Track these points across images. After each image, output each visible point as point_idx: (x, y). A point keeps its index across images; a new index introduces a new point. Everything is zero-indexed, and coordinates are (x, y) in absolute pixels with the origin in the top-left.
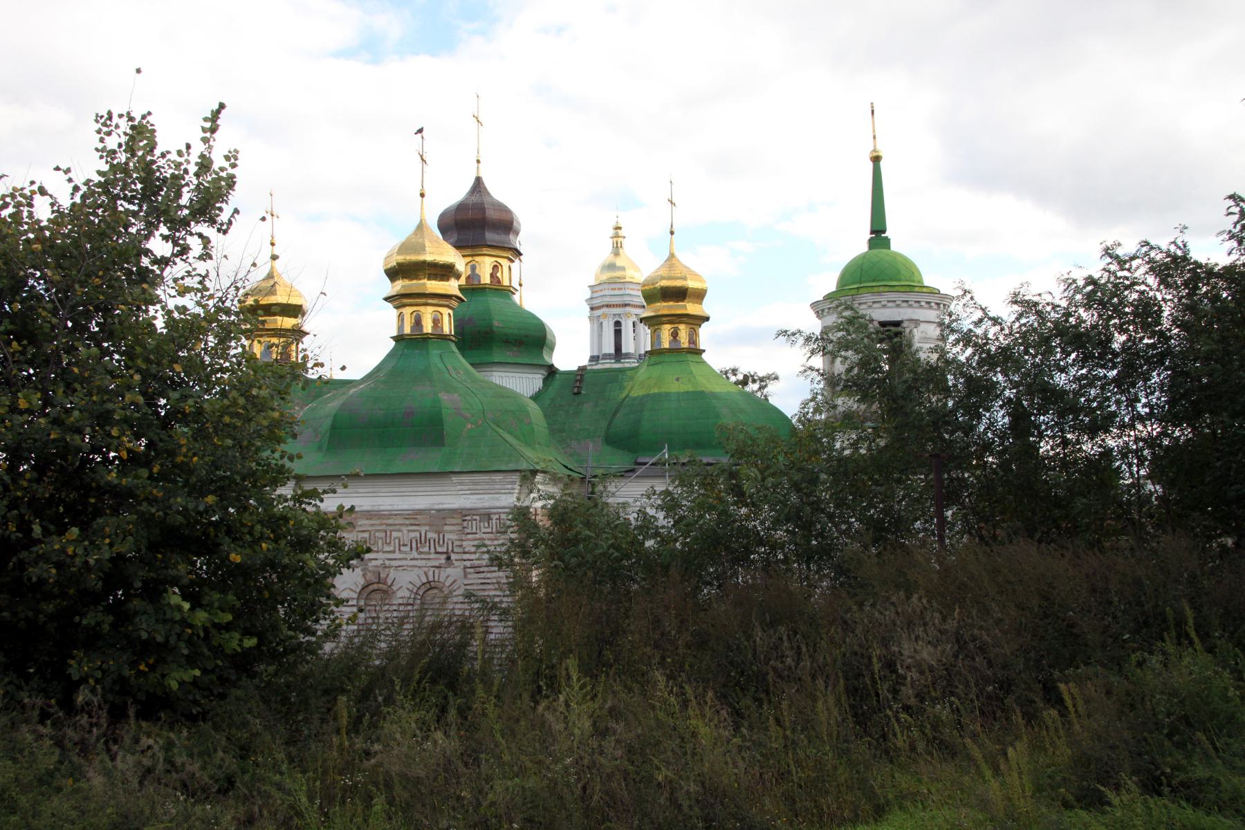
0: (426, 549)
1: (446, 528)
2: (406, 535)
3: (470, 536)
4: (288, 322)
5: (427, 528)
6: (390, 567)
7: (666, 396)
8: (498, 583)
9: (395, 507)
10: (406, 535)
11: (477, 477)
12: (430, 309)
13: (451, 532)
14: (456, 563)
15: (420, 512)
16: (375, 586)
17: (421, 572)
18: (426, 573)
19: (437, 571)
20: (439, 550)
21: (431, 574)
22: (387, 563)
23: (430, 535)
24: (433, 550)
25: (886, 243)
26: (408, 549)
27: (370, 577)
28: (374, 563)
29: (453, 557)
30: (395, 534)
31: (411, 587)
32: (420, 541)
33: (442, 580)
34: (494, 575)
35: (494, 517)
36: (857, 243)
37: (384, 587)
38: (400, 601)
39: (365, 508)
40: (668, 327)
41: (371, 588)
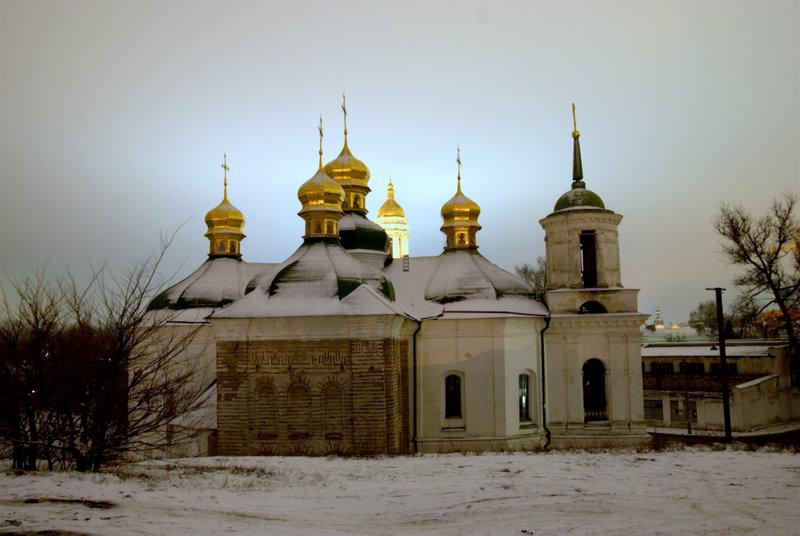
2: (318, 354)
10: (318, 354)
12: (326, 221)
25: (583, 185)
27: (295, 379)
28: (297, 371)
29: (345, 367)
36: (565, 185)
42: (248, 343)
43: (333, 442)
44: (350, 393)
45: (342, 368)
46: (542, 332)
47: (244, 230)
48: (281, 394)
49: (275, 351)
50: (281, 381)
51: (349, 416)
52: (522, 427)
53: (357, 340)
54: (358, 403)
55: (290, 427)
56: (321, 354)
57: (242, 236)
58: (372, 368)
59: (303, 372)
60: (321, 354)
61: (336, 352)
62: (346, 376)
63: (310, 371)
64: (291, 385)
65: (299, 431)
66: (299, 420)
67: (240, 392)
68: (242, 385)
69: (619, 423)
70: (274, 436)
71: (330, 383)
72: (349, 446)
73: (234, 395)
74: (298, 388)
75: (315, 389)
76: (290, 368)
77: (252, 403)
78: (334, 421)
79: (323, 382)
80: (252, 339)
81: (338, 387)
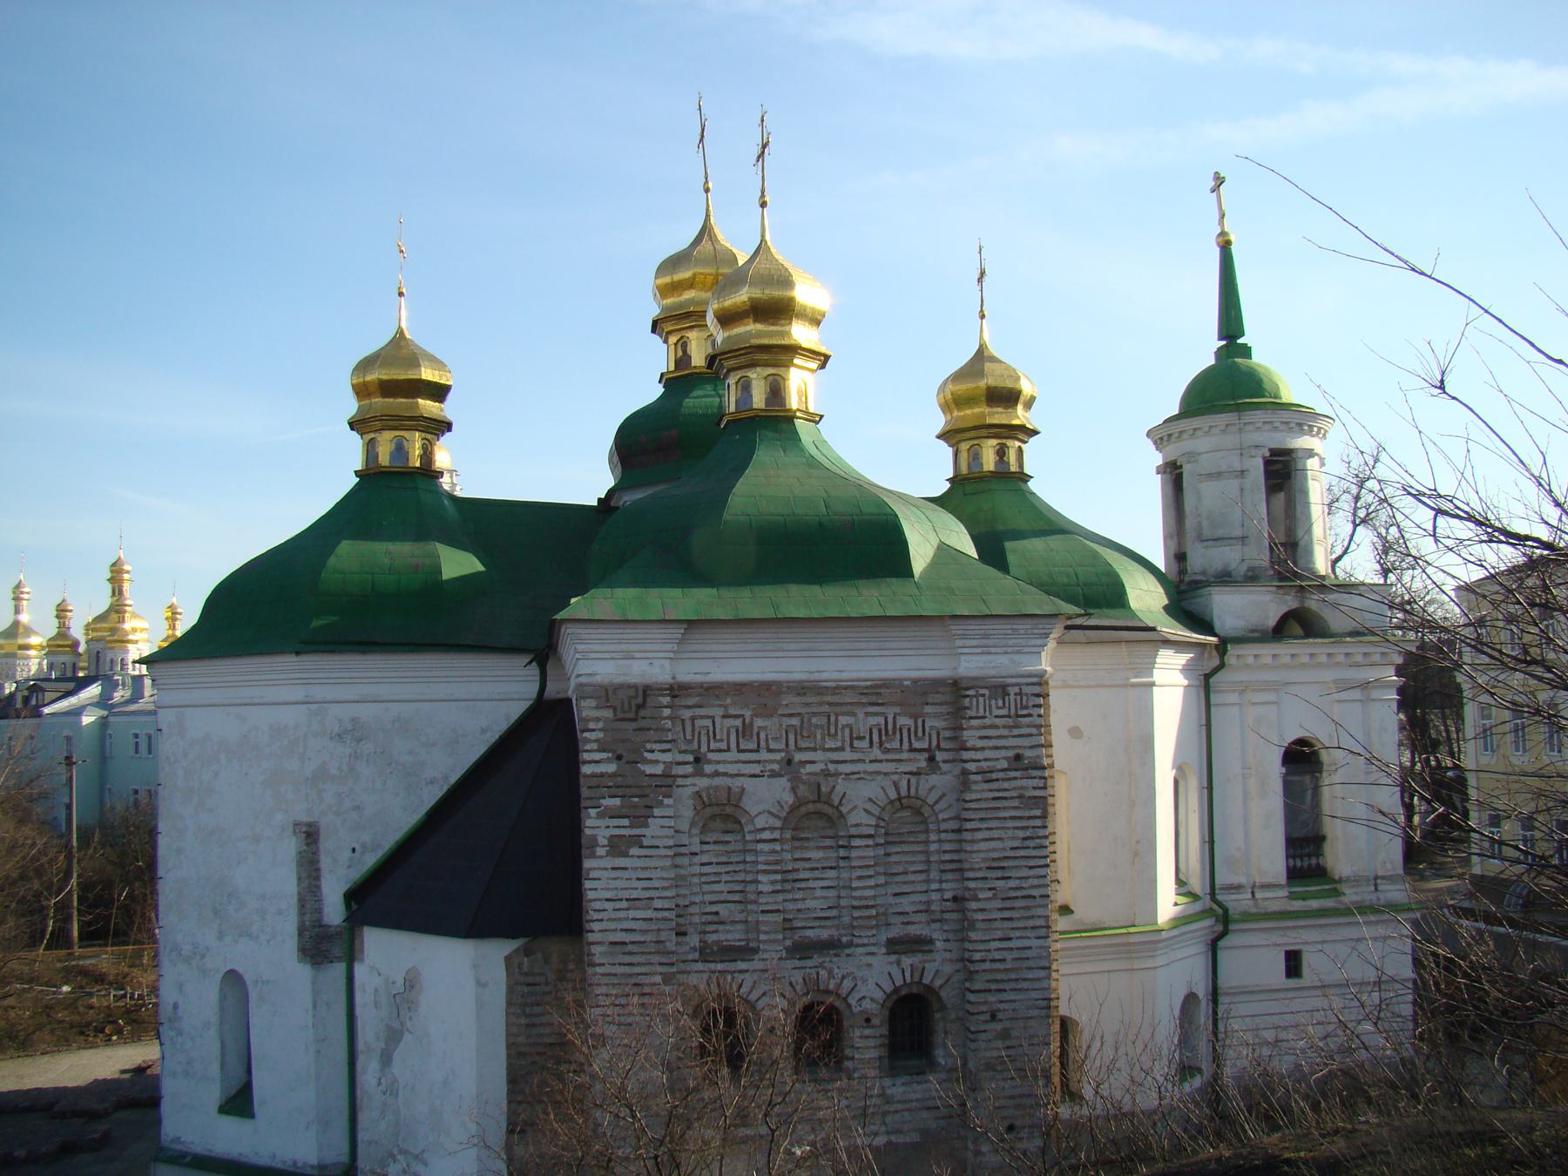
0: (896, 744)
1: (928, 709)
3: (974, 722)
4: (427, 406)
5: (898, 709)
6: (837, 774)
8: (1021, 797)
9: (845, 676)
10: (865, 721)
11: (989, 626)
13: (936, 715)
15: (886, 684)
16: (811, 807)
17: (888, 783)
18: (895, 784)
19: (913, 780)
20: (917, 745)
22: (832, 767)
23: (902, 721)
24: (906, 745)
26: (865, 744)
28: (809, 768)
29: (939, 756)
30: (843, 720)
31: (869, 806)
32: (884, 732)
33: (922, 793)
34: (1014, 784)
35: (1012, 691)
36: (1203, 352)
37: (829, 811)
38: (853, 831)
40: (994, 442)
41: (803, 810)
42: (677, 690)
43: (907, 961)
44: (953, 825)
45: (931, 759)
46: (1207, 677)
47: (447, 410)
48: (766, 835)
49: (748, 714)
50: (766, 797)
51: (950, 889)
52: (1292, 896)
53: (976, 683)
54: (981, 851)
55: (788, 926)
56: (873, 721)
57: (448, 426)
58: (1018, 757)
59: (826, 774)
60: (873, 721)
61: (915, 717)
63: (843, 768)
64: (793, 809)
65: (808, 933)
66: (810, 904)
67: (654, 829)
68: (656, 812)
69: (1356, 881)
70: (745, 951)
71: (900, 803)
72: (948, 969)
73: (637, 841)
74: (815, 813)
75: (859, 819)
76: (789, 762)
77: (685, 861)
78: (906, 904)
79: (883, 801)
80: (683, 678)
81: (918, 812)
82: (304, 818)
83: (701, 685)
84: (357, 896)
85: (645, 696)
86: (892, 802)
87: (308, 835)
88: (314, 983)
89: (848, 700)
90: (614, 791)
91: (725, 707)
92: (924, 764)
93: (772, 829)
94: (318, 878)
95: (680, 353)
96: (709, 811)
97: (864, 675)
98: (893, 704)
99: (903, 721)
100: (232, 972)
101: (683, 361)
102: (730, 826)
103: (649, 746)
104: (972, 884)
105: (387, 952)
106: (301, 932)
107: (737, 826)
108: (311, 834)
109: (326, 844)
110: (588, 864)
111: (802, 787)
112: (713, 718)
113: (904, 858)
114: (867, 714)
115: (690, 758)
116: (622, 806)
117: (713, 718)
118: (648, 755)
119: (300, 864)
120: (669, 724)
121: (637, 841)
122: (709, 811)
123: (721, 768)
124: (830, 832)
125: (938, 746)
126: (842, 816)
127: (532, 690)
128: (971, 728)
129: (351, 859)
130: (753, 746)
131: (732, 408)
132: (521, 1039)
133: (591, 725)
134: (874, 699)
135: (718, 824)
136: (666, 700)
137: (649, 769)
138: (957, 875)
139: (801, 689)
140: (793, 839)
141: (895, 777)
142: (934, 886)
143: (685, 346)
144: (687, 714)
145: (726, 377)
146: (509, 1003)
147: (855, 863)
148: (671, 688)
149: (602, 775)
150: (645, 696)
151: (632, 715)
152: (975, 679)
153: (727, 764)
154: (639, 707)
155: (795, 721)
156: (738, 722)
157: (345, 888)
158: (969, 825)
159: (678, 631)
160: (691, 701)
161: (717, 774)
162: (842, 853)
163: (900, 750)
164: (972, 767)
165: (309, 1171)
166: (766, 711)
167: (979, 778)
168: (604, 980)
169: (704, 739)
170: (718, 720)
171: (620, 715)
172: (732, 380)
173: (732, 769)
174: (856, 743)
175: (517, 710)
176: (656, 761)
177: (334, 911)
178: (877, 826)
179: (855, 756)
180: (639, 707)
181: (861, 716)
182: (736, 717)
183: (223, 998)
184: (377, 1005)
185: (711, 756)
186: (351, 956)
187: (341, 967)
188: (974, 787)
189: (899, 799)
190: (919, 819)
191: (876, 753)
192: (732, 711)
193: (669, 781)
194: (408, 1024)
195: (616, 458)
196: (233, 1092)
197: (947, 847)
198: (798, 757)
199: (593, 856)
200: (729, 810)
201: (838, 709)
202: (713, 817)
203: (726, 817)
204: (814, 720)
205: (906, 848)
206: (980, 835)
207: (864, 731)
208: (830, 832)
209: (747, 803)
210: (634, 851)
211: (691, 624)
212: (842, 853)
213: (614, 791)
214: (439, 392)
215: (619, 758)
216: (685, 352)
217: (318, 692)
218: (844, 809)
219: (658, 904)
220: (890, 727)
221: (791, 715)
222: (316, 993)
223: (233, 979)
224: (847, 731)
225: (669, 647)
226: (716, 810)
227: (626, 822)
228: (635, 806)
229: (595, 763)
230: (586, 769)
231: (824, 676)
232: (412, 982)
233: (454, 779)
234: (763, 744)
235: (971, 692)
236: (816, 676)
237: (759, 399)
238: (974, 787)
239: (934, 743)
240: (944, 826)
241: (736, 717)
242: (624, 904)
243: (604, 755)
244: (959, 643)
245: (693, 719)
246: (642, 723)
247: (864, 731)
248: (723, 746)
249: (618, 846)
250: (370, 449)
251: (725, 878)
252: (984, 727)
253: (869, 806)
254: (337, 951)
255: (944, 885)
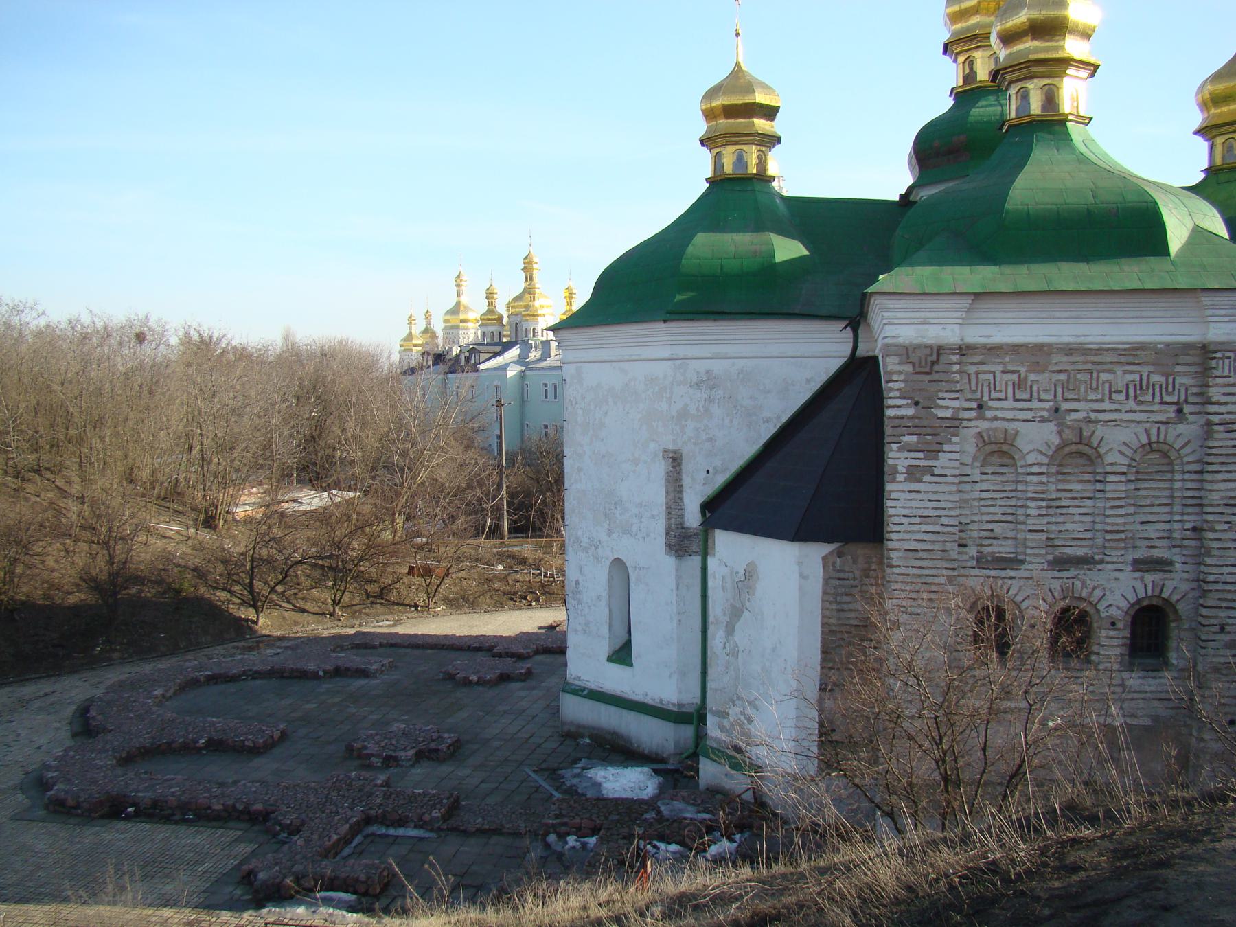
0: (1149, 398)
1: (1178, 369)
2: (1123, 378)
3: (1219, 381)
4: (761, 124)
5: (1151, 369)
6: (1097, 422)
7: (931, 263)
9: (1107, 339)
10: (1123, 378)
13: (1185, 374)
14: (1191, 418)
15: (1142, 347)
16: (1074, 448)
17: (1140, 429)
18: (1147, 431)
19: (1163, 428)
20: (1167, 399)
21: (1154, 432)
22: (1093, 416)
23: (1156, 378)
24: (1157, 399)
26: (1122, 397)
27: (1068, 434)
28: (1074, 416)
29: (1187, 409)
31: (1124, 449)
32: (1139, 387)
33: (1170, 439)
38: (1109, 469)
39: (1065, 340)
41: (1067, 450)
42: (964, 350)
43: (1149, 578)
44: (1196, 467)
45: (1180, 411)
48: (1035, 469)
49: (1023, 370)
50: (1035, 440)
51: (1191, 520)
55: (1050, 543)
56: (1129, 377)
60: (1129, 377)
61: (1167, 375)
62: (1188, 430)
64: (1059, 448)
65: (1068, 550)
66: (1069, 527)
67: (943, 462)
68: (946, 447)
70: (1013, 562)
71: (1150, 447)
72: (1185, 587)
73: (929, 470)
74: (1078, 453)
75: (1114, 459)
76: (1057, 410)
77: (968, 487)
80: (970, 339)
81: (1165, 455)
82: (671, 447)
83: (984, 346)
84: (709, 506)
85: (938, 354)
86: (1143, 446)
87: (674, 459)
88: (677, 570)
89: (1109, 360)
90: (912, 430)
91: (1004, 364)
92: (1172, 415)
93: (1041, 464)
94: (681, 492)
95: (967, 71)
96: (988, 448)
97: (1124, 339)
98: (1147, 364)
99: (1156, 378)
100: (618, 559)
101: (970, 77)
102: (1006, 461)
103: (940, 395)
104: (1210, 518)
105: (732, 549)
106: (667, 534)
107: (1010, 461)
108: (675, 460)
109: (687, 466)
110: (889, 487)
111: (1067, 431)
112: (994, 373)
113: (1152, 493)
114: (1125, 372)
115: (975, 405)
116: (918, 443)
117: (994, 373)
118: (940, 402)
119: (668, 481)
120: (957, 377)
121: (929, 470)
122: (988, 448)
123: (999, 414)
124: (1089, 469)
125: (1186, 401)
126: (1100, 456)
127: (846, 349)
128: (1217, 385)
129: (706, 479)
130: (1027, 396)
131: (1013, 115)
132: (833, 621)
133: (895, 378)
134: (1131, 359)
135: (995, 459)
136: (955, 358)
137: (940, 413)
138: (1197, 510)
139: (1069, 350)
140: (1058, 473)
141: (1148, 425)
142: (1177, 517)
143: (971, 64)
144: (972, 369)
145: (1007, 89)
146: (825, 593)
147: (1108, 495)
148: (960, 348)
149: (902, 417)
150: (938, 354)
151: (928, 370)
152: (1223, 343)
153: (1006, 412)
154: (934, 363)
155: (1063, 377)
156: (1015, 377)
157: (701, 500)
158: (1210, 468)
159: (967, 302)
160: (976, 359)
161: (996, 418)
162: (1099, 486)
163: (1152, 403)
164: (1215, 419)
165: (671, 708)
166: (1037, 368)
167: (1221, 428)
168: (900, 578)
169: (986, 390)
170: (998, 374)
171: (918, 370)
172: (1012, 91)
173: (1009, 415)
174: (1114, 396)
175: (834, 365)
176: (946, 407)
177: (693, 518)
178: (1129, 465)
179: (1113, 407)
180: (934, 363)
181: (1119, 373)
182: (1013, 372)
183: (611, 579)
184: (724, 588)
185: (991, 403)
186: (705, 553)
187: (697, 560)
188: (1216, 436)
189: (1150, 444)
190: (1166, 461)
191: (1132, 404)
192: (1010, 368)
193: (956, 423)
194: (747, 604)
195: (914, 161)
196: (617, 647)
197: (1189, 485)
198: (1065, 406)
199: (894, 481)
200: (1005, 448)
201: (1099, 367)
202: (992, 453)
203: (1004, 454)
204: (1079, 376)
205: (1153, 485)
206: (1219, 477)
207: (1121, 386)
208: (1089, 469)
209: (1019, 442)
210: (927, 478)
211: (977, 295)
212: (1099, 486)
213: (912, 430)
214: (770, 112)
215: (917, 404)
216: (971, 69)
217: (681, 351)
218: (1102, 451)
219: (945, 521)
220: (1144, 383)
221: (1060, 371)
222: (678, 577)
223: (618, 563)
224: (1107, 385)
225: (959, 315)
226: (994, 447)
227: (921, 455)
228: (927, 443)
229: (896, 407)
230: (889, 412)
231: (1089, 339)
232: (751, 572)
233: (785, 418)
234: (1035, 394)
235: (1218, 355)
236: (1081, 340)
237: (1036, 107)
238: (1216, 436)
239: (1183, 397)
240: (1188, 468)
241: (1013, 372)
242: (918, 520)
243: (904, 402)
244: (1209, 312)
245: (977, 373)
246: (936, 377)
247: (1121, 386)
248: (1002, 395)
249: (914, 474)
250: (717, 159)
251: (999, 502)
252: (1229, 385)
253: (1124, 449)
254: (694, 547)
255: (1186, 517)
